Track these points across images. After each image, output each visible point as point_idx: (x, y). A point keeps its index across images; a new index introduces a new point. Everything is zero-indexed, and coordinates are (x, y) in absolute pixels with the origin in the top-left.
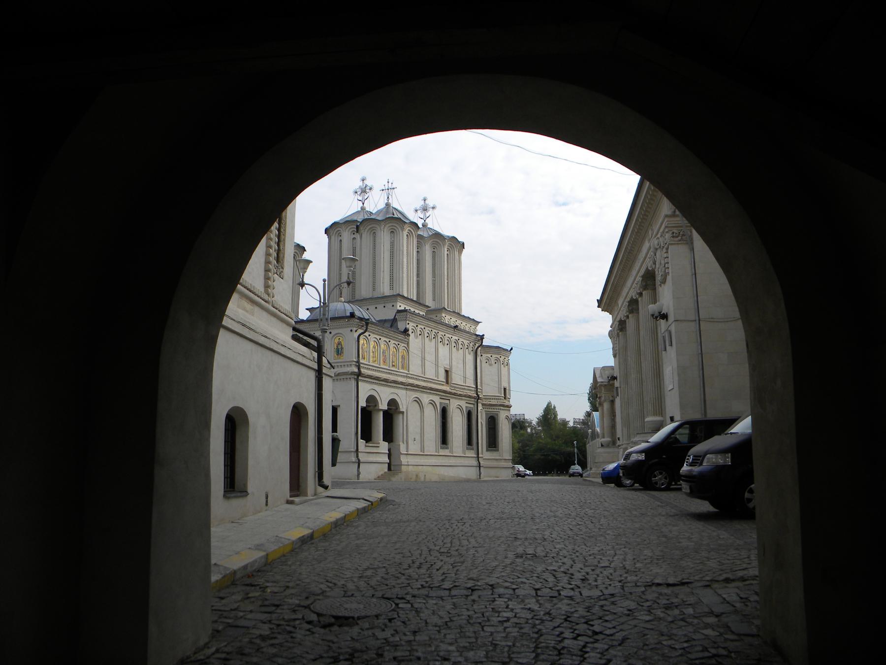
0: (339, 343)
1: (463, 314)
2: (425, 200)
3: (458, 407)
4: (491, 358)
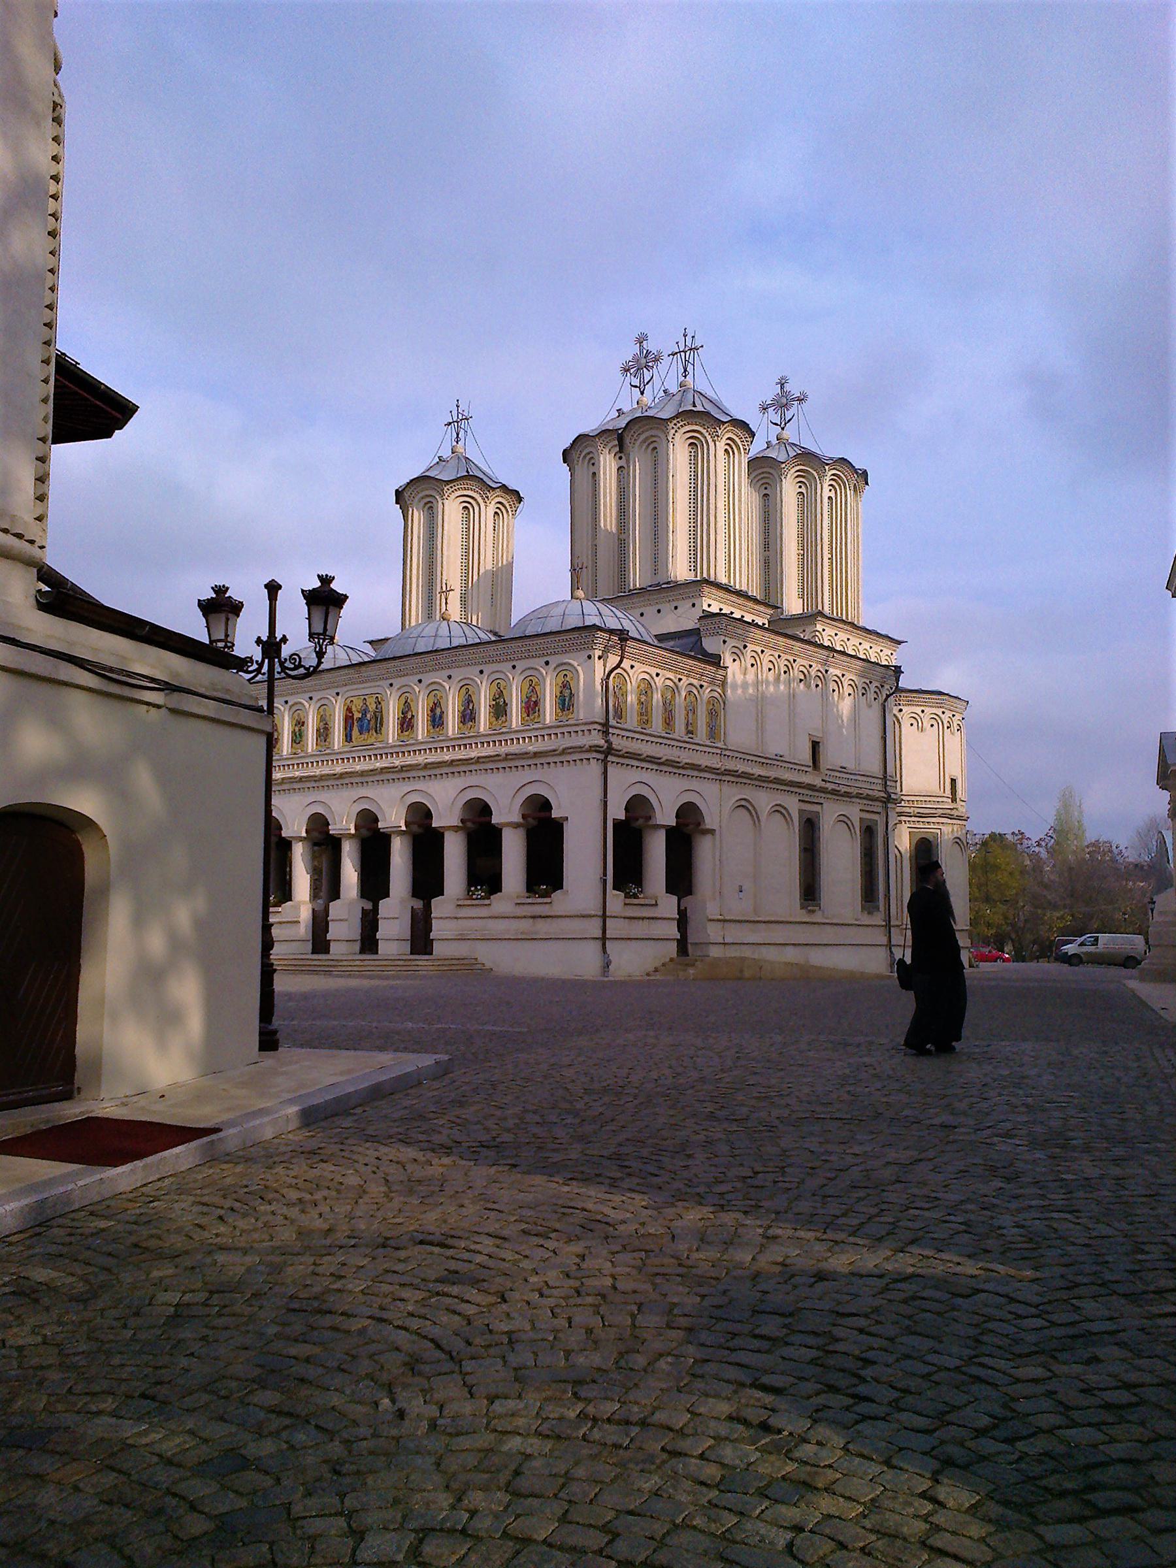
1: (861, 624)
2: (782, 386)
3: (842, 818)
4: (922, 715)
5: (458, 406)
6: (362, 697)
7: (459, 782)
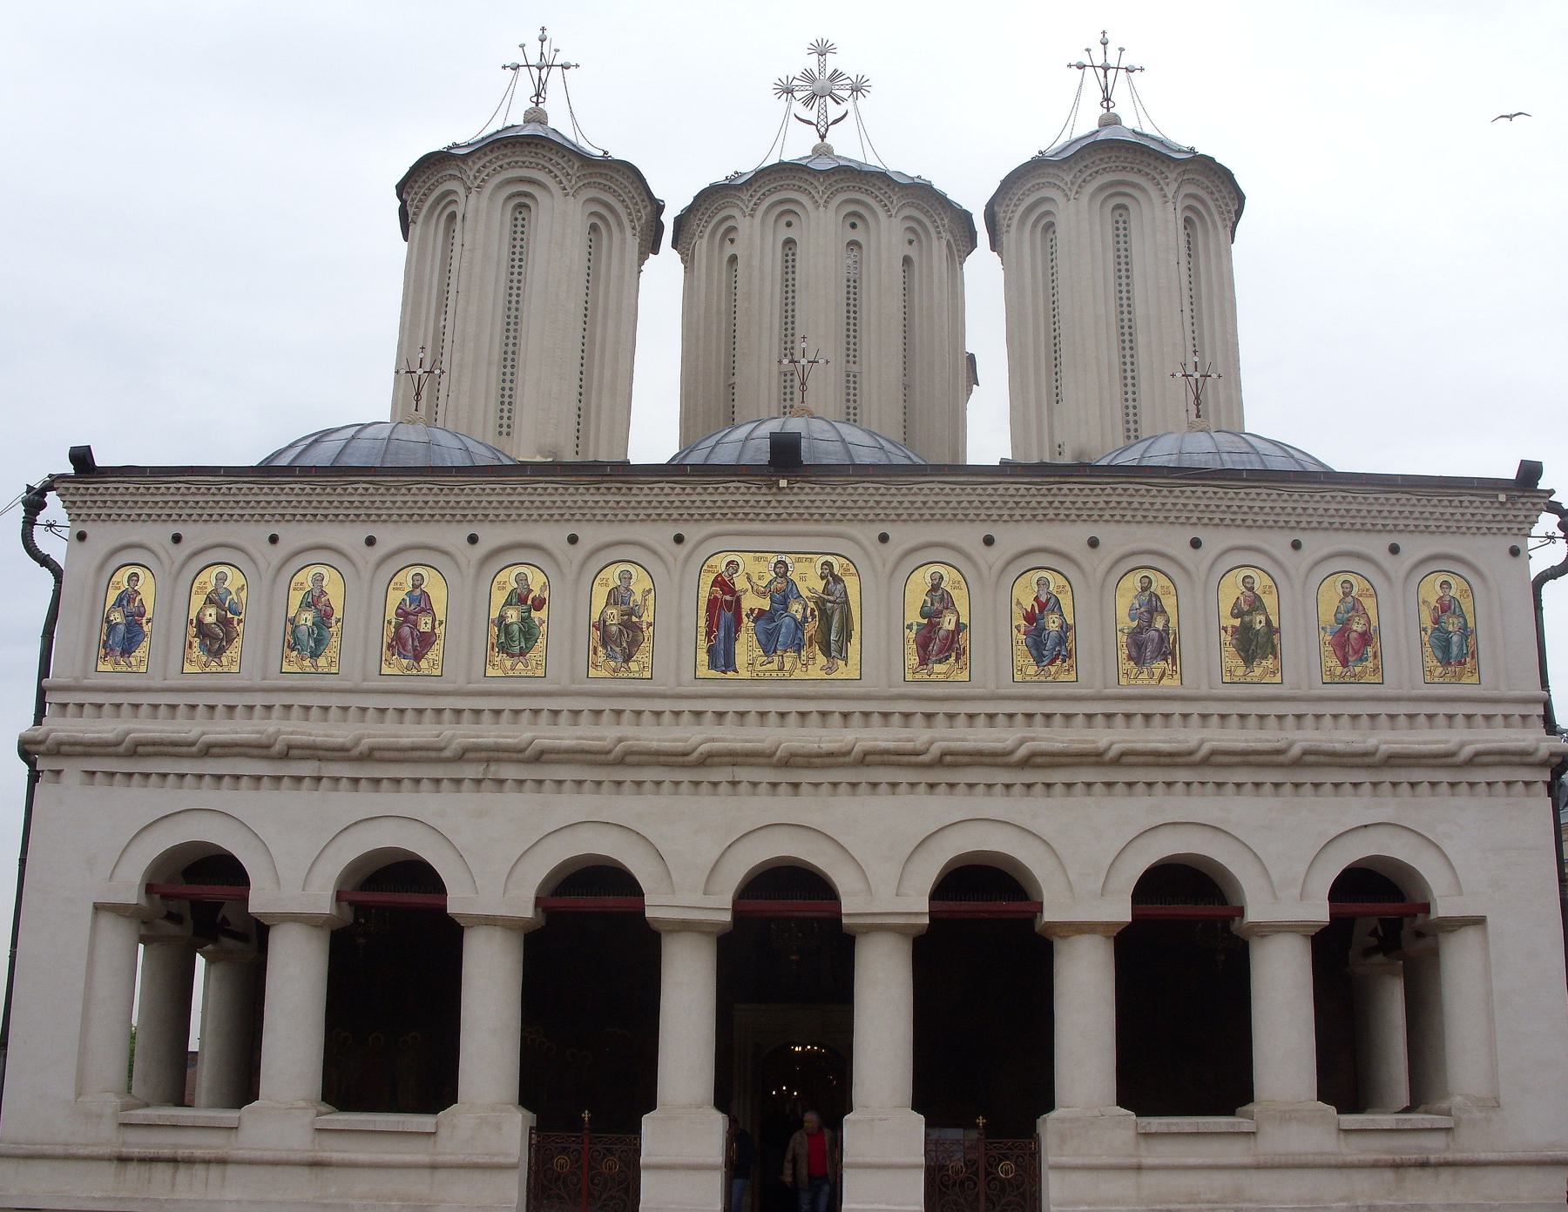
0: (1446, 607)
5: (542, 40)
6: (774, 559)
7: (1137, 811)
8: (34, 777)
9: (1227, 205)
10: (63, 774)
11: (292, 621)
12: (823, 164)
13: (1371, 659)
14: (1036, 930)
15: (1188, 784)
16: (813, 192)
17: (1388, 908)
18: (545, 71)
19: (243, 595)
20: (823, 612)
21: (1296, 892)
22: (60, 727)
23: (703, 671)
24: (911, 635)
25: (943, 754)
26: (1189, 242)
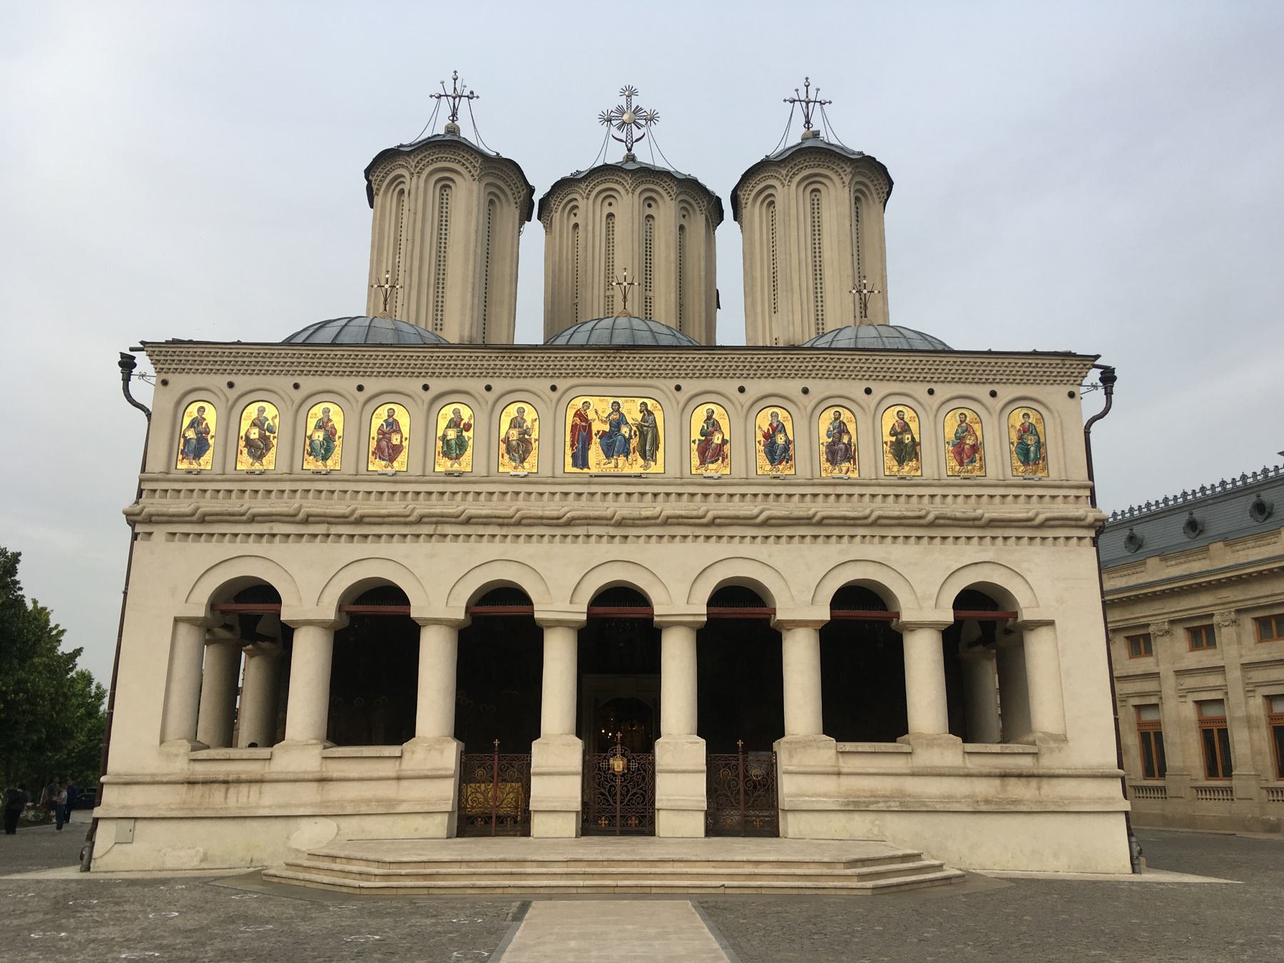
0: (1027, 430)
5: (455, 80)
6: (611, 400)
7: (832, 552)
8: (135, 537)
9: (881, 188)
10: (153, 535)
11: (310, 437)
12: (630, 166)
13: (978, 461)
14: (771, 625)
15: (864, 537)
16: (625, 184)
17: (989, 614)
18: (457, 99)
19: (277, 421)
20: (641, 433)
21: (933, 603)
22: (153, 505)
23: (569, 468)
24: (695, 447)
25: (715, 518)
26: (857, 212)
